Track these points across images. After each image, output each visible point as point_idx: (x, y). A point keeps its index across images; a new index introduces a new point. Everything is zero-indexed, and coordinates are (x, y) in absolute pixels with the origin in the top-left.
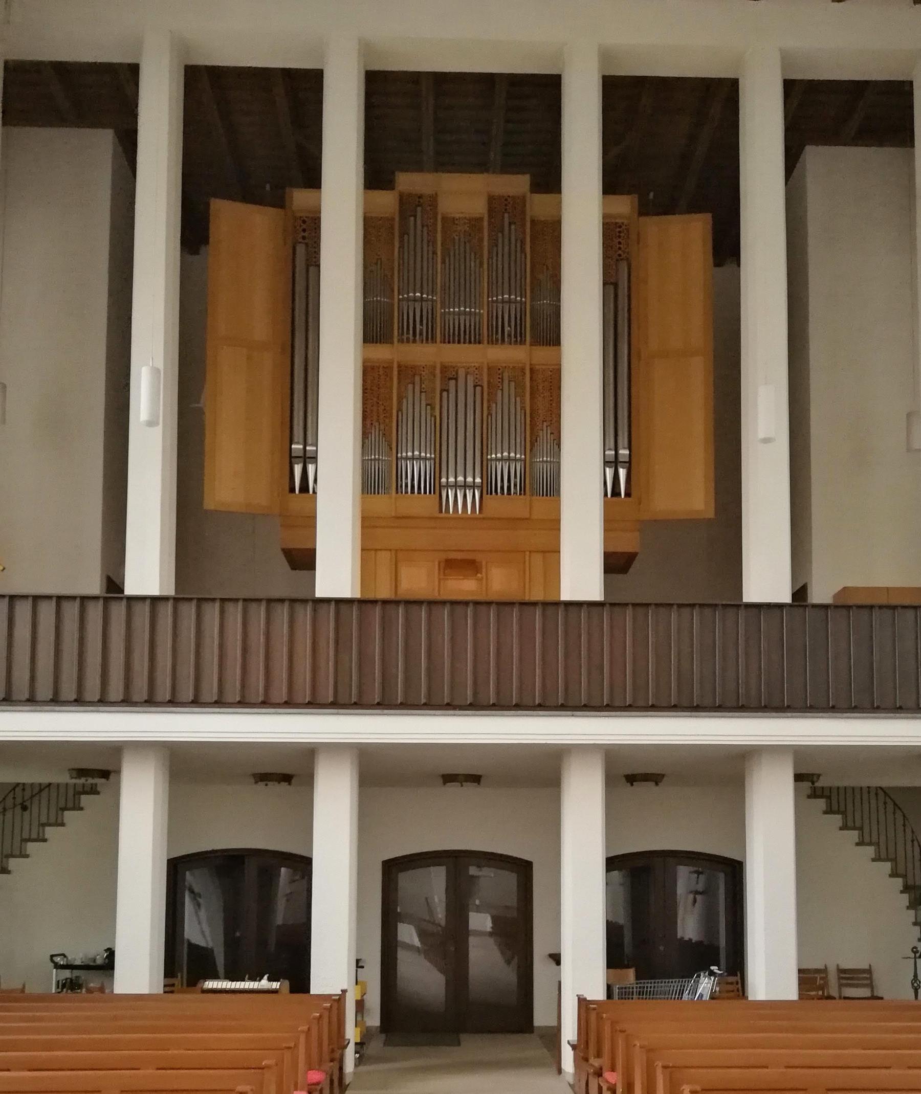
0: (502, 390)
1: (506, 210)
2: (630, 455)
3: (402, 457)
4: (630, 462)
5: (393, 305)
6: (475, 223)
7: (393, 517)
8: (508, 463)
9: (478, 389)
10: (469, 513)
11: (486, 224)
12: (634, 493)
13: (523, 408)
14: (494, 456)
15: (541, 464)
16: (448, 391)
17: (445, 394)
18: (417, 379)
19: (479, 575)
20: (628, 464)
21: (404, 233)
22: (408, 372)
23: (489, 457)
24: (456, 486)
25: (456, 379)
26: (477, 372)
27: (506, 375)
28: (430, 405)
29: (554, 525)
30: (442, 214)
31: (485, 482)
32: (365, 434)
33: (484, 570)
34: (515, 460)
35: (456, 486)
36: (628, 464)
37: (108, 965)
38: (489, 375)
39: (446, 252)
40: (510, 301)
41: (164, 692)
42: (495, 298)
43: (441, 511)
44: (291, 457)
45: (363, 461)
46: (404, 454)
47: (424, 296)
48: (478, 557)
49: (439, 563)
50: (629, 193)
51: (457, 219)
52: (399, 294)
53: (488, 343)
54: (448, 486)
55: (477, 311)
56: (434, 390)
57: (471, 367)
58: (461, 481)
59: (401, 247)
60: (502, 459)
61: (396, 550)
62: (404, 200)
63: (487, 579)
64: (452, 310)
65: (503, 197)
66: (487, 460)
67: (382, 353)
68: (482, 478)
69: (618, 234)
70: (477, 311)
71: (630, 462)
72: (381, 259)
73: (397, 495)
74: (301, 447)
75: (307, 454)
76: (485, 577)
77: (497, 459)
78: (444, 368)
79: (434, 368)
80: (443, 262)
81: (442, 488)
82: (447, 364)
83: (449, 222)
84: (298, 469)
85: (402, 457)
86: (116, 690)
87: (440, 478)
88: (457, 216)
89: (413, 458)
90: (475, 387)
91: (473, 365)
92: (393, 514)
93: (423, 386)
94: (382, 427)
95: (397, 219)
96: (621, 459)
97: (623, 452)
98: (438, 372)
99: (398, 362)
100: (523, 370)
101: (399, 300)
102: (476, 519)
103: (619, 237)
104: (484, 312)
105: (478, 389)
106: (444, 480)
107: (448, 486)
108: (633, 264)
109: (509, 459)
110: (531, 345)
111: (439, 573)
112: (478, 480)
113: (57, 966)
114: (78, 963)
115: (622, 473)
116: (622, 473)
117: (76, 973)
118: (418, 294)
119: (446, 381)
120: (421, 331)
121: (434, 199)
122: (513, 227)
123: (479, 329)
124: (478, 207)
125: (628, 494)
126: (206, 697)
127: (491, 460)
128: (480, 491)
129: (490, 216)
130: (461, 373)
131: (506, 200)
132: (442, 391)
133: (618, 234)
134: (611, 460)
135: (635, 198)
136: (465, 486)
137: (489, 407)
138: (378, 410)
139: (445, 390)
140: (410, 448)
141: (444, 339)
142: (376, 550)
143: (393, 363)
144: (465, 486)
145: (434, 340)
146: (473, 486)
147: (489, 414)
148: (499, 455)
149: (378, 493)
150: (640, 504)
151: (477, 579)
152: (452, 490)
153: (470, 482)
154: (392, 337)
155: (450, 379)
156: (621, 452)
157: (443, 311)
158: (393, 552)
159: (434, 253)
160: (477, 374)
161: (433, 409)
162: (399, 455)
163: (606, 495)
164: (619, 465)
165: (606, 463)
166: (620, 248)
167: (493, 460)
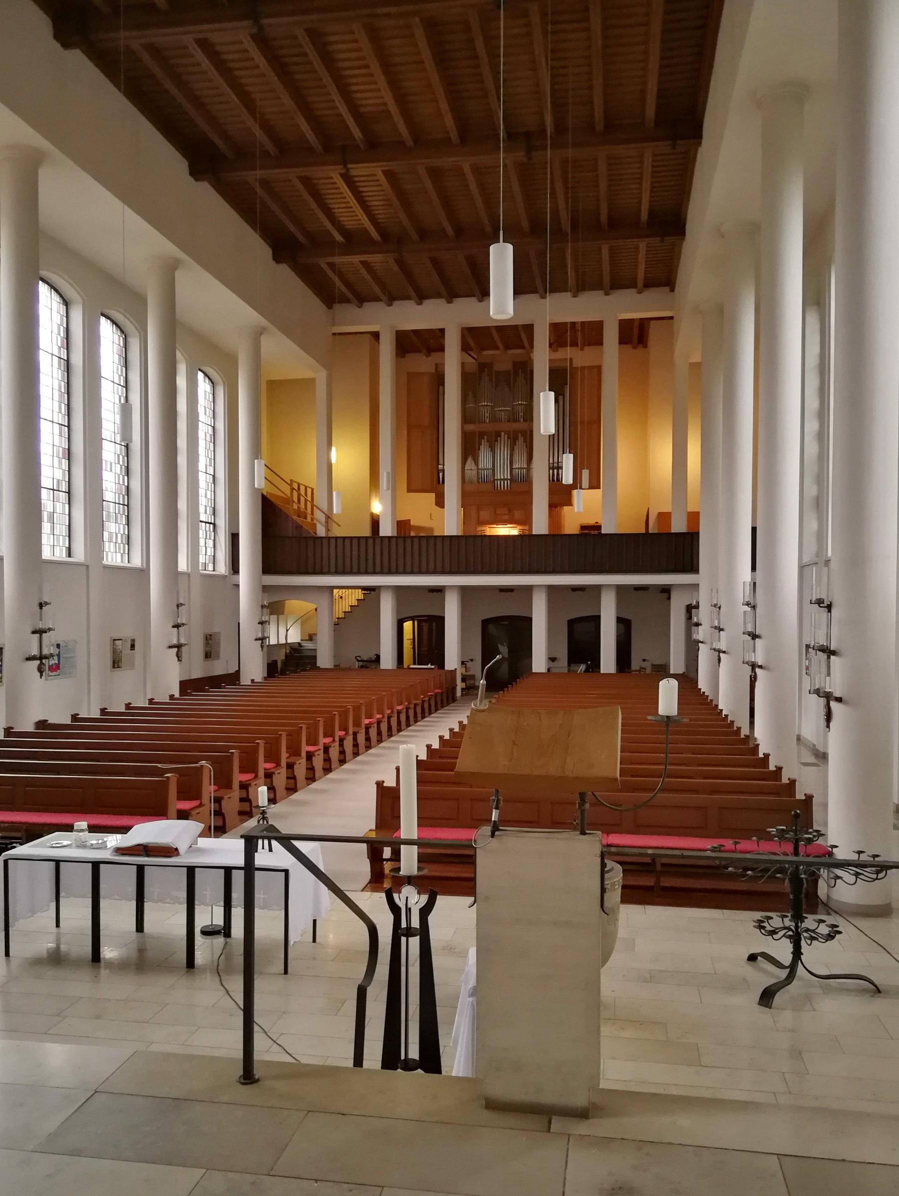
13: (526, 447)
22: (482, 435)
37: (378, 658)
67: (470, 427)
77: (516, 468)
78: (496, 432)
84: (441, 475)
100: (526, 431)
107: (497, 480)
113: (358, 661)
114: (365, 659)
117: (365, 663)
130: (503, 434)
146: (507, 479)
163: (550, 481)
165: (550, 468)
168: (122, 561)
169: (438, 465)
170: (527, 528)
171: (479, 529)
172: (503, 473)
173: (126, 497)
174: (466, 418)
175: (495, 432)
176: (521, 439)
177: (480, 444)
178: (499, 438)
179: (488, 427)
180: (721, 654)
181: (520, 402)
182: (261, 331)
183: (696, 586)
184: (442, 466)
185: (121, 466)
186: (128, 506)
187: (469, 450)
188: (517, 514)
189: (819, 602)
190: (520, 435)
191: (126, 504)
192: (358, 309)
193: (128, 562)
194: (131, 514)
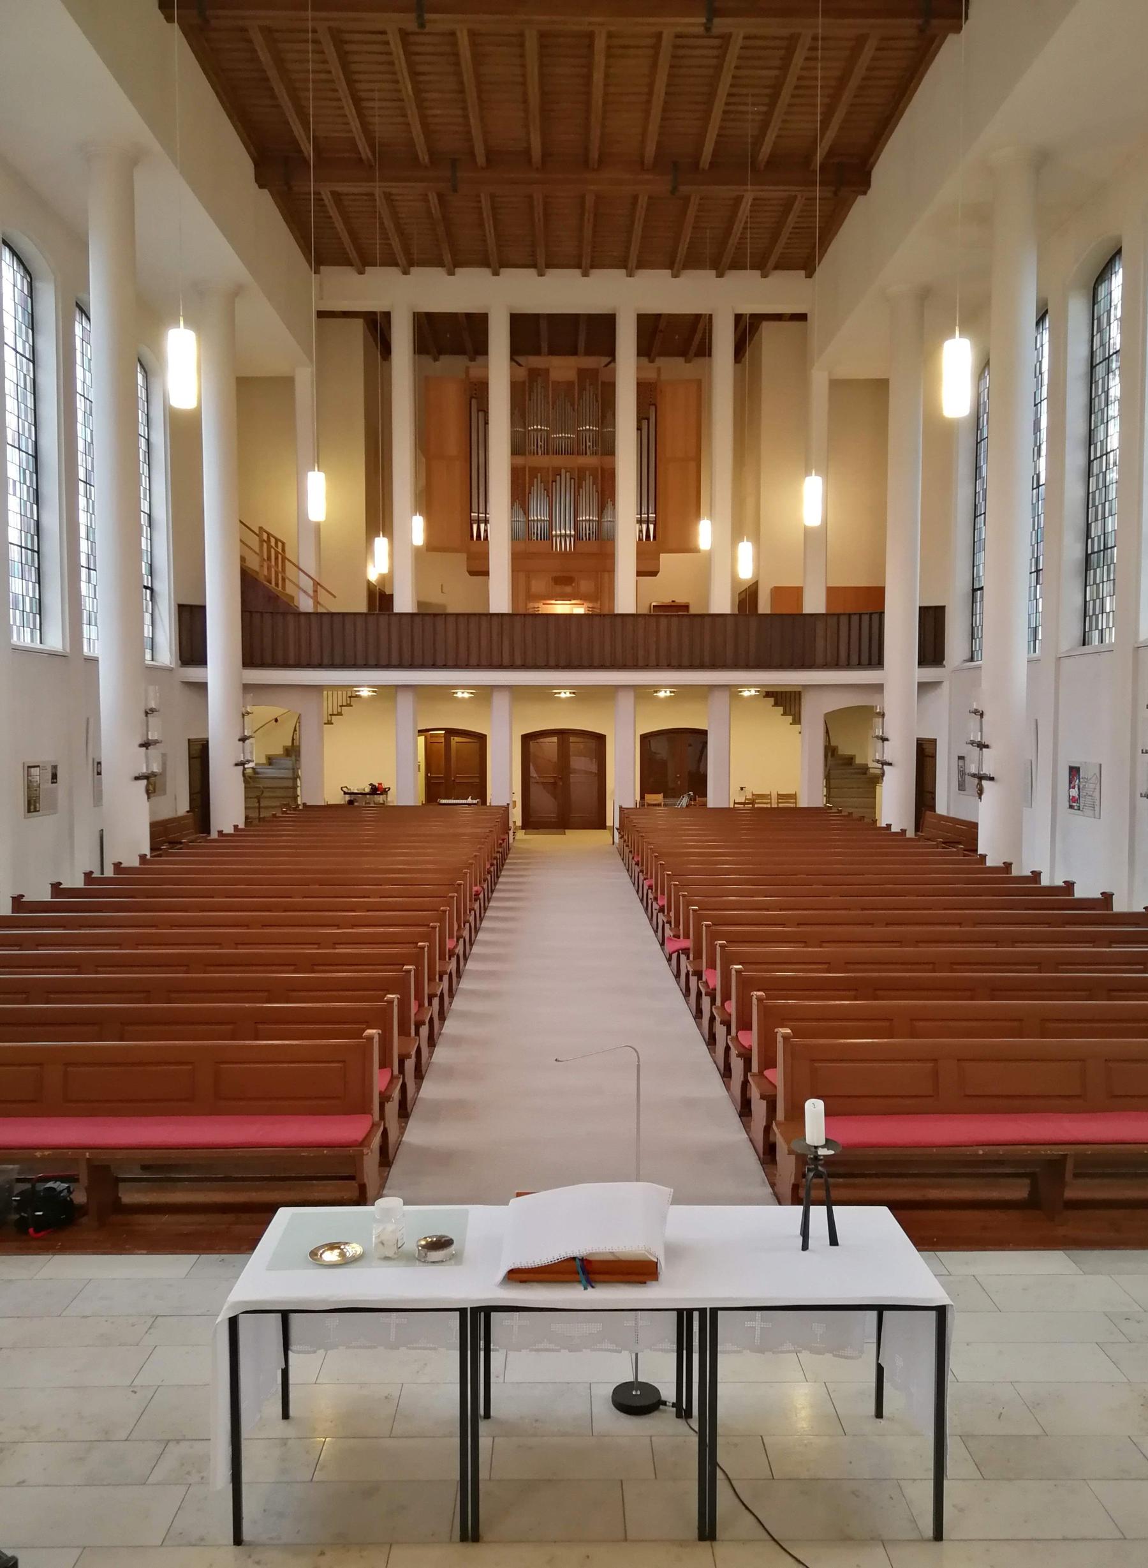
4: (655, 521)
6: (570, 384)
9: (572, 481)
13: (597, 491)
16: (555, 481)
17: (554, 483)
18: (539, 475)
22: (534, 471)
32: (512, 505)
34: (593, 520)
39: (554, 403)
44: (471, 520)
45: (512, 521)
56: (549, 482)
60: (586, 520)
71: (655, 521)
74: (476, 514)
77: (583, 520)
79: (548, 469)
80: (553, 408)
84: (475, 527)
89: (537, 520)
90: (571, 479)
96: (650, 519)
100: (597, 469)
105: (572, 481)
106: (554, 533)
107: (556, 536)
109: (589, 520)
110: (602, 455)
112: (573, 533)
115: (651, 527)
118: (539, 427)
120: (541, 446)
121: (547, 370)
124: (572, 375)
130: (563, 471)
132: (553, 481)
145: (548, 454)
146: (570, 536)
147: (579, 495)
159: (548, 403)
168: (32, 641)
169: (471, 512)
170: (598, 605)
171: (531, 605)
172: (563, 530)
173: (36, 537)
174: (517, 449)
175: (554, 468)
176: (588, 482)
177: (531, 484)
178: (558, 477)
179: (542, 461)
180: (984, 783)
181: (588, 427)
182: (237, 291)
183: (879, 688)
184: (476, 514)
185: (28, 487)
186: (38, 552)
187: (520, 496)
188: (585, 586)
189: (976, 712)
190: (587, 473)
191: (36, 549)
192: (356, 274)
193: (41, 643)
194: (44, 568)
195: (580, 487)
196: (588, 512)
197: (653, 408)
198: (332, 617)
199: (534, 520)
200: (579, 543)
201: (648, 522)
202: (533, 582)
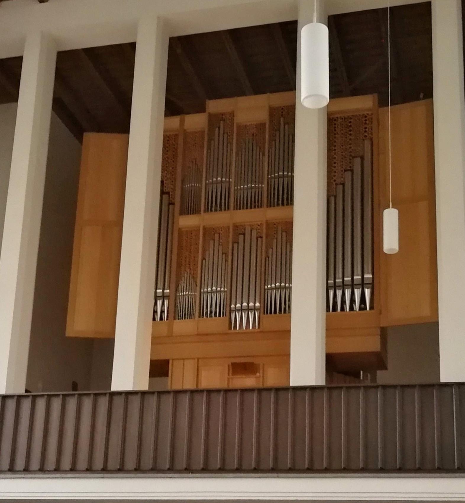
0: (277, 239)
1: (282, 115)
2: (373, 278)
3: (204, 292)
4: (373, 284)
5: (201, 189)
6: (261, 126)
7: (196, 335)
8: (279, 291)
9: (259, 239)
10: (244, 328)
11: (267, 126)
12: (375, 306)
14: (269, 286)
15: (270, 291)
16: (238, 243)
17: (236, 245)
18: (217, 236)
19: (258, 374)
20: (371, 286)
21: (210, 140)
23: (266, 287)
24: (242, 310)
25: (244, 234)
26: (259, 227)
27: (280, 228)
28: (225, 254)
29: (286, 333)
30: (237, 124)
31: (262, 305)
33: (261, 371)
35: (242, 310)
36: (371, 286)
38: (267, 229)
40: (283, 176)
41: (147, 462)
42: (276, 175)
43: (230, 328)
46: (205, 290)
47: (224, 179)
48: (256, 361)
49: (229, 366)
50: (371, 93)
51: (248, 126)
52: (206, 180)
53: (267, 207)
54: (236, 310)
55: (260, 185)
57: (255, 224)
58: (239, 307)
59: (209, 148)
60: (276, 288)
61: (198, 359)
62: (211, 117)
63: (263, 377)
64: (242, 187)
65: (280, 107)
66: (265, 289)
68: (260, 303)
69: (364, 122)
70: (260, 185)
72: (196, 159)
73: (200, 319)
75: (165, 294)
76: (262, 376)
77: (271, 289)
79: (228, 228)
80: (237, 154)
81: (231, 312)
82: (237, 224)
83: (242, 128)
85: (204, 292)
86: (82, 462)
87: (231, 305)
88: (248, 124)
91: (256, 223)
92: (196, 333)
93: (221, 240)
94: (192, 272)
95: (206, 130)
97: (368, 276)
98: (231, 230)
99: (204, 226)
101: (206, 184)
102: (251, 333)
103: (366, 123)
104: (265, 186)
106: (233, 306)
107: (236, 310)
108: (375, 141)
109: (280, 287)
111: (228, 375)
112: (258, 304)
115: (367, 292)
116: (367, 292)
119: (237, 236)
121: (232, 115)
122: (286, 126)
123: (261, 198)
124: (263, 116)
125: (371, 308)
126: (144, 466)
127: (268, 289)
128: (259, 313)
129: (271, 121)
131: (282, 109)
132: (233, 243)
133: (364, 122)
134: (359, 283)
135: (376, 95)
136: (248, 309)
137: (267, 253)
138: (190, 260)
139: (235, 242)
140: (210, 284)
141: (208, 208)
142: (184, 359)
143: (199, 227)
144: (248, 309)
146: (255, 309)
148: (273, 285)
149: (190, 318)
150: (380, 313)
151: (255, 377)
152: (238, 313)
153: (251, 306)
154: (200, 211)
155: (240, 234)
156: (366, 276)
157: (236, 188)
158: (196, 360)
159: (231, 150)
160: (259, 229)
161: (227, 256)
162: (202, 290)
164: (365, 286)
166: (366, 132)
167: (273, 289)
178: (241, 237)
195: (269, 246)
196: (283, 278)
197: (367, 143)
198: (159, 398)
199: (207, 292)
200: (265, 317)
201: (363, 285)
202: (204, 374)
